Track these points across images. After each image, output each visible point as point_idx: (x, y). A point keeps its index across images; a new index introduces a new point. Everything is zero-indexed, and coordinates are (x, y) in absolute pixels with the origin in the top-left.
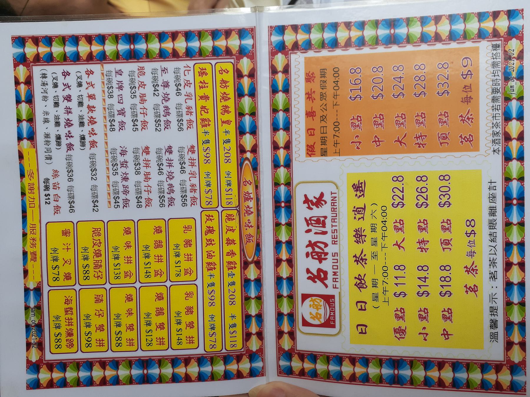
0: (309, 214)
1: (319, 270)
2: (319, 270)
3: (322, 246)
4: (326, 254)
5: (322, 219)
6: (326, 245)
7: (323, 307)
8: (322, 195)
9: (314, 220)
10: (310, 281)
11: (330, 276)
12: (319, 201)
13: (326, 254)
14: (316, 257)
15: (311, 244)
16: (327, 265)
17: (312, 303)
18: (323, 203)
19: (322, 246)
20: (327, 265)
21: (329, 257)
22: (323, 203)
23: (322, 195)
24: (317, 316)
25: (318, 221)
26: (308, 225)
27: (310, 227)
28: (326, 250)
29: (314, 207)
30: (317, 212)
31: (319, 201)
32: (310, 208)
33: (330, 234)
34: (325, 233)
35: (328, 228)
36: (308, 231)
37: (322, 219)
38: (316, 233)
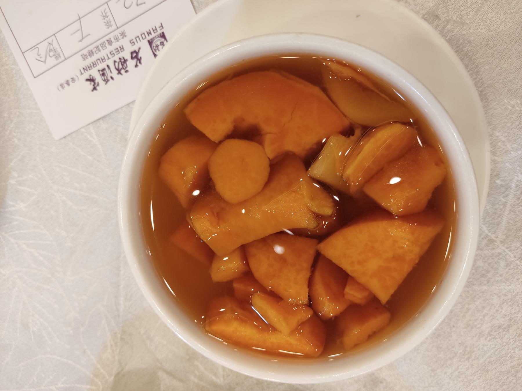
0: (102, 83)
5: (101, 73)
6: (115, 62)
8: (87, 80)
10: (142, 61)
12: (91, 80)
15: (119, 72)
17: (157, 51)
23: (87, 80)
25: (103, 75)
26: (108, 80)
29: (96, 82)
30: (98, 78)
31: (91, 80)
32: (98, 84)
34: (108, 66)
37: (101, 73)
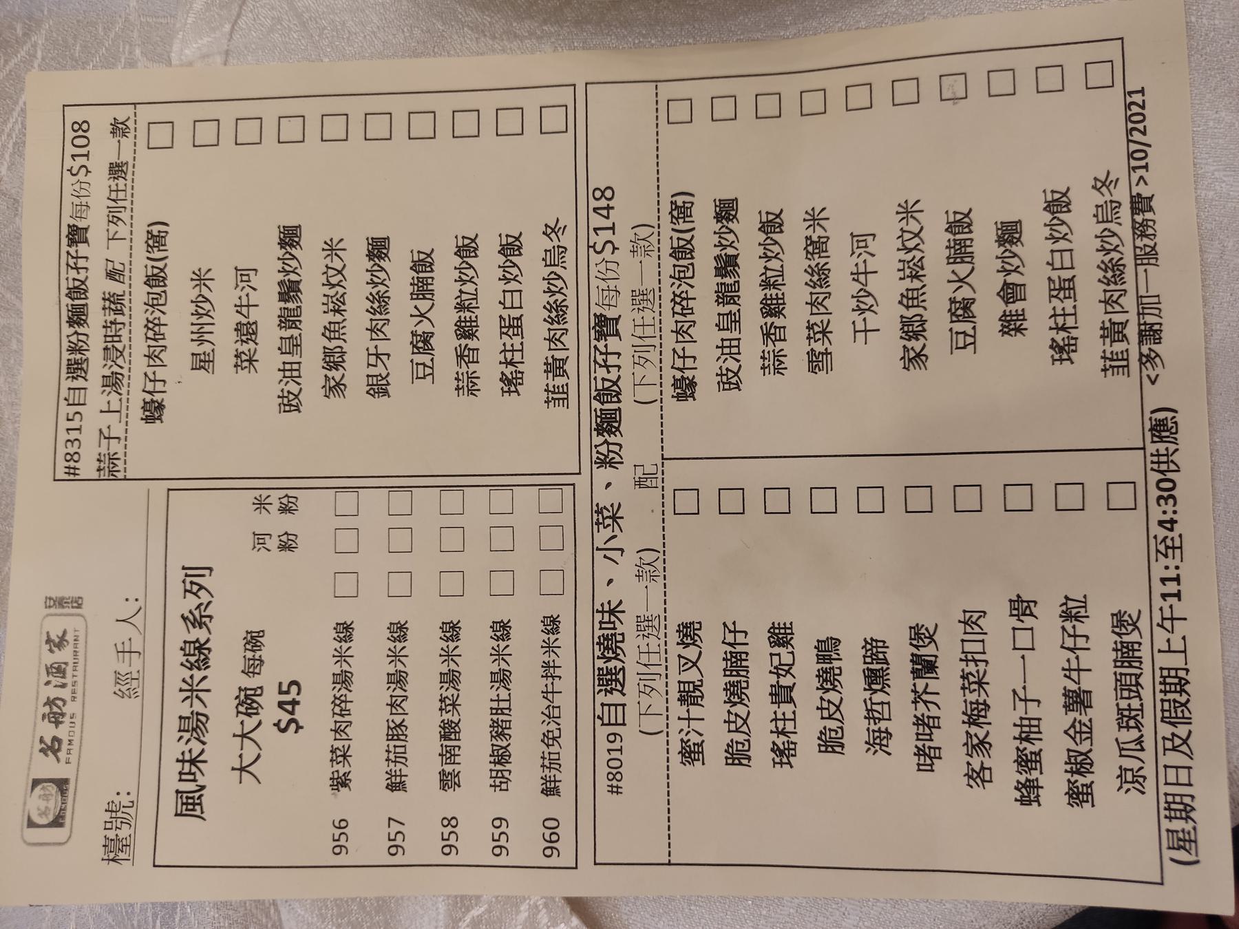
1: (55, 739)
2: (55, 739)
3: (60, 703)
4: (63, 715)
7: (54, 797)
9: (54, 668)
11: (65, 746)
13: (63, 715)
14: (53, 719)
16: (62, 732)
17: (42, 793)
18: (65, 643)
19: (60, 703)
20: (62, 732)
21: (67, 719)
22: (65, 643)
24: (43, 814)
27: (51, 678)
28: (64, 709)
33: (69, 688)
34: (63, 686)
35: (69, 680)
36: (48, 683)
38: (56, 686)
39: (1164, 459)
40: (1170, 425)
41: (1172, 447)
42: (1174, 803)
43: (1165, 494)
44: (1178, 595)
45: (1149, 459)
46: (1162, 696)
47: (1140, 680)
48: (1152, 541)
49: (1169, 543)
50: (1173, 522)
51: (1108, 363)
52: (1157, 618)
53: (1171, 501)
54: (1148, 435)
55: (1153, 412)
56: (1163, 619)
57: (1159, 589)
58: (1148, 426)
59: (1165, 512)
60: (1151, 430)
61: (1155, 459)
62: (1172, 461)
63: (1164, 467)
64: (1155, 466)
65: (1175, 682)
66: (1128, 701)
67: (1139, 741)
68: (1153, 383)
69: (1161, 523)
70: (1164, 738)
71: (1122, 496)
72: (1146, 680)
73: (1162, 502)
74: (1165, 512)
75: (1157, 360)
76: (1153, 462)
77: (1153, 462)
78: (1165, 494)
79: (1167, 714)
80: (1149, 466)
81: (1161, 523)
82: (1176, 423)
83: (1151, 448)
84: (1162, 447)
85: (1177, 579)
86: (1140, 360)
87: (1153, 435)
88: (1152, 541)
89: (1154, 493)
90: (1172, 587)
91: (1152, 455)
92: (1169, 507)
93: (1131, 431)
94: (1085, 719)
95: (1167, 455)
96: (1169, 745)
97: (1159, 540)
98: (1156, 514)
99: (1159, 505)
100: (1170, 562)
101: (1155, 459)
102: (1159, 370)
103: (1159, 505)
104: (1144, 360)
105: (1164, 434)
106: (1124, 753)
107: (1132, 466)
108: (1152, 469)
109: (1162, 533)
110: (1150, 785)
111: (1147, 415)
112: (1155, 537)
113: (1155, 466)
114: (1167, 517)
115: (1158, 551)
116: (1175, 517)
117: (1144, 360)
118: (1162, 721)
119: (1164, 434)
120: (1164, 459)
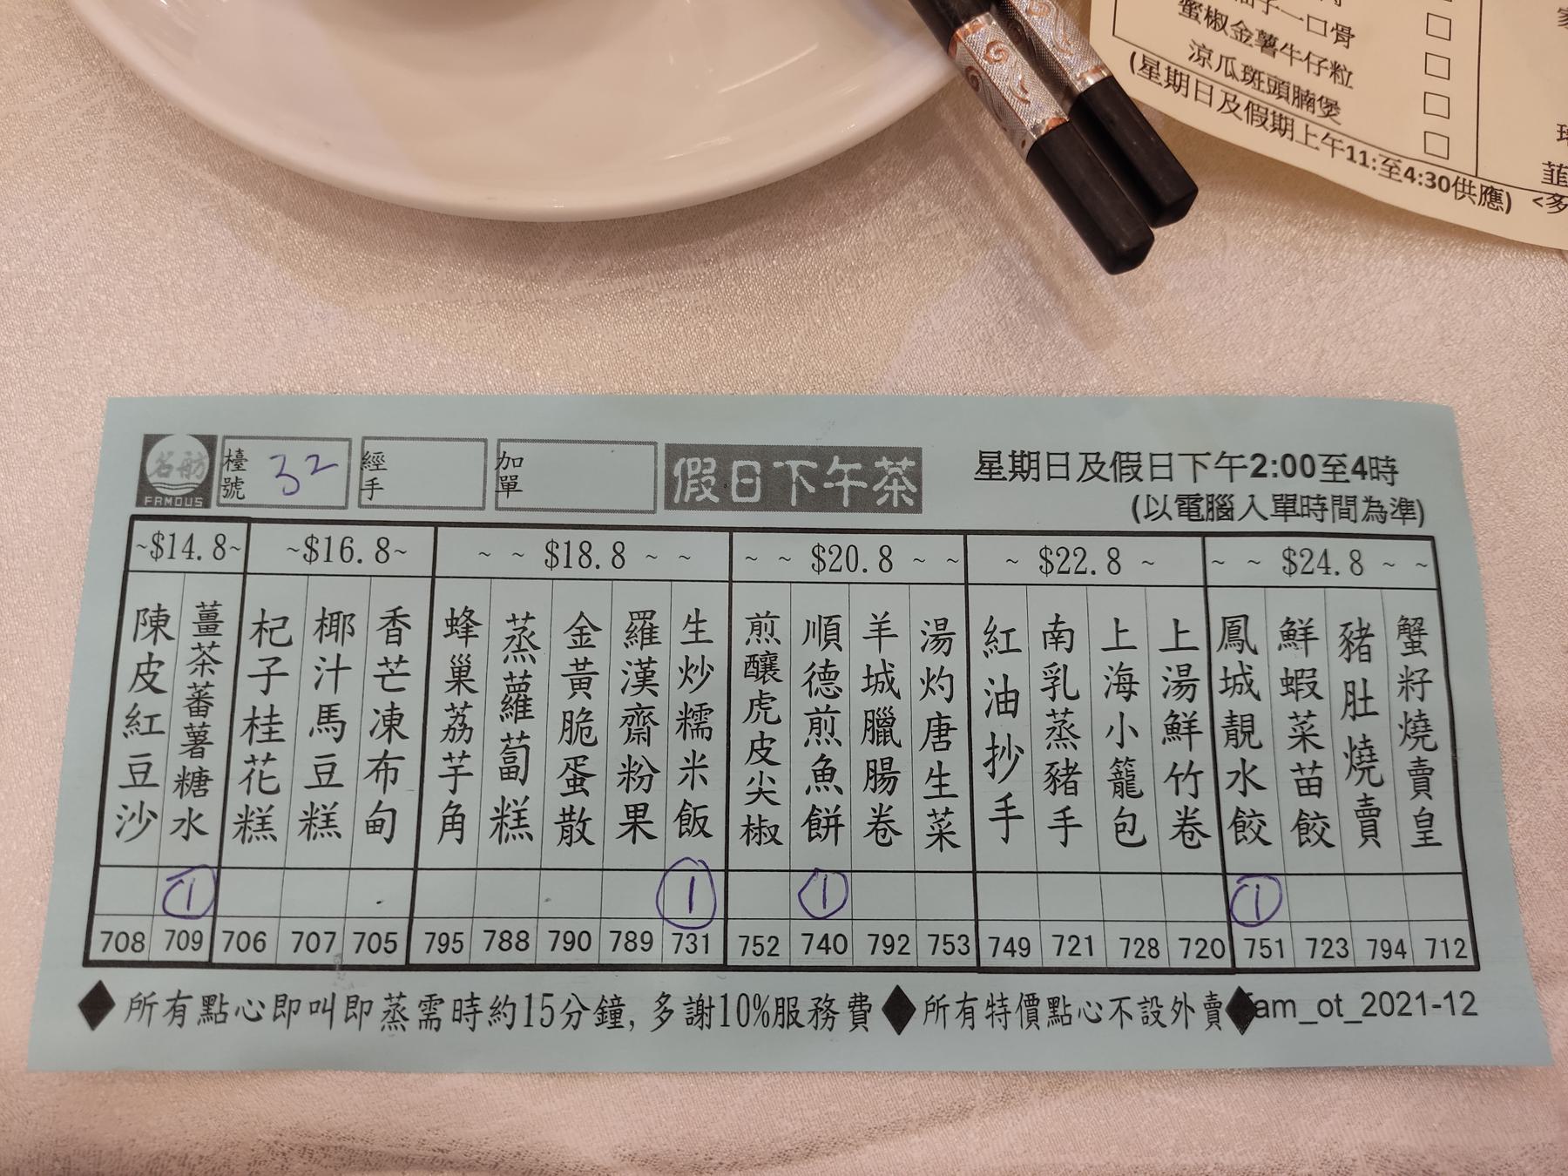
39: (1467, 189)
40: (1496, 204)
41: (1477, 199)
42: (1181, 80)
43: (1436, 181)
44: (1351, 159)
45: (1468, 178)
46: (1271, 110)
47: (1283, 99)
48: (1397, 158)
49: (1394, 170)
50: (1413, 179)
51: (1556, 169)
52: (1333, 135)
53: (1430, 184)
54: (1489, 184)
55: (1508, 193)
56: (1333, 140)
57: (1359, 148)
58: (1496, 186)
59: (1421, 175)
60: (1492, 187)
61: (1467, 183)
62: (1463, 196)
63: (1460, 187)
64: (1461, 181)
65: (1282, 126)
66: (1266, 81)
67: (1233, 75)
68: (1535, 200)
69: (1411, 169)
70: (1235, 97)
71: (1438, 146)
72: (1282, 103)
73: (1430, 176)
74: (1421, 175)
75: (1556, 209)
76: (1464, 180)
77: (1464, 180)
78: (1436, 181)
79: (1255, 108)
80: (1462, 176)
81: (1411, 169)
82: (1497, 209)
83: (1477, 183)
84: (1477, 191)
85: (1364, 164)
86: (1557, 195)
87: (1488, 188)
88: (1397, 158)
89: (1439, 173)
90: (1359, 158)
91: (1471, 182)
92: (1424, 179)
93: (1493, 171)
94: (1251, 41)
95: (1469, 193)
96: (1230, 98)
97: (1398, 164)
98: (1420, 168)
99: (1428, 173)
100: (1379, 164)
101: (1467, 183)
102: (1546, 208)
103: (1428, 173)
104: (1557, 198)
105: (1488, 197)
106: (1224, 60)
107: (1462, 161)
108: (1458, 178)
109: (1404, 168)
110: (1196, 66)
111: (1506, 189)
112: (1399, 161)
113: (1461, 181)
114: (1416, 175)
115: (1388, 159)
116: (1416, 182)
117: (1557, 198)
118: (1250, 102)
119: (1488, 197)
120: (1467, 189)
